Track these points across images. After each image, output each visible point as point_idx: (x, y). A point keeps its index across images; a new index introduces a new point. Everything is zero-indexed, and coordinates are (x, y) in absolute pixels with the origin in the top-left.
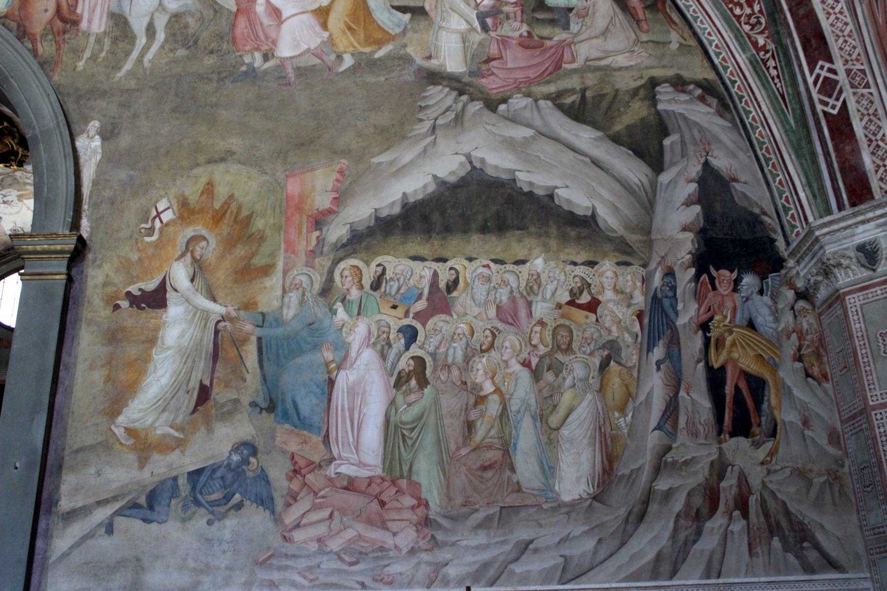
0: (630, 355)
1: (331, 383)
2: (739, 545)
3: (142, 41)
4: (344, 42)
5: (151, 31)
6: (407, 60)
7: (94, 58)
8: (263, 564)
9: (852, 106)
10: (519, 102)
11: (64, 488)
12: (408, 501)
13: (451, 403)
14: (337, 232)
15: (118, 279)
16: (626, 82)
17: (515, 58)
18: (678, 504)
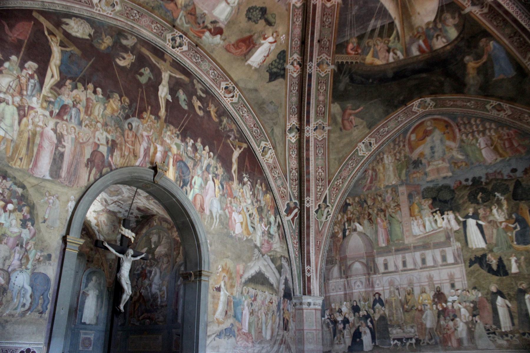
0: (275, 313)
1: (242, 313)
2: (284, 349)
3: (215, 220)
4: (245, 233)
5: (216, 217)
6: (252, 240)
7: (207, 222)
8: (234, 348)
9: (312, 277)
10: (266, 256)
11: (208, 330)
12: (251, 338)
13: (256, 319)
14: (243, 280)
15: (213, 283)
16: (279, 256)
17: (266, 245)
18: (279, 342)
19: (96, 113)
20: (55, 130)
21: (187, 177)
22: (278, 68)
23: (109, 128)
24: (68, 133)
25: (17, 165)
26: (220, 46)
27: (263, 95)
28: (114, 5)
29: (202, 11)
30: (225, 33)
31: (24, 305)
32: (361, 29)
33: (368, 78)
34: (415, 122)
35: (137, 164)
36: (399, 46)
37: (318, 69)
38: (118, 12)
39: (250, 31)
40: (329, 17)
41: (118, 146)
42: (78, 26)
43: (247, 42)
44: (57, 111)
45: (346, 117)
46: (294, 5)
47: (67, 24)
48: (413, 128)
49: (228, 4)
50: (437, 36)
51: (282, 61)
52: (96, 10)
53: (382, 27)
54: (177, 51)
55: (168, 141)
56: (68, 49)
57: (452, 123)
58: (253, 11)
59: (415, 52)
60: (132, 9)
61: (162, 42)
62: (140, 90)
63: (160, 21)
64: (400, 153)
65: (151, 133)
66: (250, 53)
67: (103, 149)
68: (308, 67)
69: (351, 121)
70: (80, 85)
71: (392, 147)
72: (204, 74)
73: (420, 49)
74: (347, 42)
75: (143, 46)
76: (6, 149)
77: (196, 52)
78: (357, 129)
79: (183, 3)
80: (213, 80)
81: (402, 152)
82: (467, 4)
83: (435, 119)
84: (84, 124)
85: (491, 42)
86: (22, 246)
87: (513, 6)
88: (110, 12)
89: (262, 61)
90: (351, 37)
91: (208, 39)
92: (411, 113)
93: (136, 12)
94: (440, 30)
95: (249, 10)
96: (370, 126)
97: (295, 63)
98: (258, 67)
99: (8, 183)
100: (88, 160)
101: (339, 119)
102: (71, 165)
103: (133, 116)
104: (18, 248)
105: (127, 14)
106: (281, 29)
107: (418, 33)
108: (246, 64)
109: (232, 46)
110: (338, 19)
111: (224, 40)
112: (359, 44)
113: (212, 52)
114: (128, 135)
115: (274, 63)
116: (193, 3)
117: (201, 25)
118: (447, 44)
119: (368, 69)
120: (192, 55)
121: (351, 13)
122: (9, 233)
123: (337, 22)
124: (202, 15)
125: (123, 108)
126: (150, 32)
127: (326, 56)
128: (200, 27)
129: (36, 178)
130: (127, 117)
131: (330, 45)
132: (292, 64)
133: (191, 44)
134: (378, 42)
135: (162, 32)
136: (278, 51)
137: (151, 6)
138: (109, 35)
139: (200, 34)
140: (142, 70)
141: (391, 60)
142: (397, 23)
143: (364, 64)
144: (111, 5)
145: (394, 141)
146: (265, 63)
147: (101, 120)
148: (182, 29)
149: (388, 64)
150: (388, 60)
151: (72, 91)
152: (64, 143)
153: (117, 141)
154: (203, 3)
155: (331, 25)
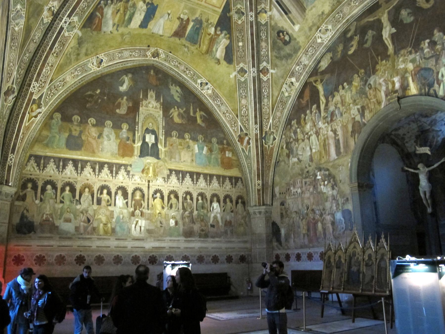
19: (347, 100)
20: (332, 130)
21: (431, 79)
23: (357, 101)
24: (338, 126)
25: (323, 161)
31: (343, 228)
35: (383, 106)
38: (332, 28)
41: (366, 107)
44: (330, 119)
52: (326, 42)
55: (402, 66)
56: (324, 80)
60: (334, 17)
62: (369, 53)
65: (386, 75)
67: (358, 118)
70: (336, 93)
75: (361, 20)
76: (317, 157)
84: (343, 113)
86: (335, 199)
88: (331, 33)
93: (337, 15)
99: (323, 172)
100: (352, 132)
102: (344, 142)
103: (369, 77)
104: (334, 201)
105: (336, 21)
114: (370, 93)
122: (328, 195)
125: (362, 79)
129: (331, 162)
130: (366, 81)
140: (366, 38)
144: (326, 31)
147: (351, 101)
151: (332, 101)
152: (337, 133)
153: (365, 105)
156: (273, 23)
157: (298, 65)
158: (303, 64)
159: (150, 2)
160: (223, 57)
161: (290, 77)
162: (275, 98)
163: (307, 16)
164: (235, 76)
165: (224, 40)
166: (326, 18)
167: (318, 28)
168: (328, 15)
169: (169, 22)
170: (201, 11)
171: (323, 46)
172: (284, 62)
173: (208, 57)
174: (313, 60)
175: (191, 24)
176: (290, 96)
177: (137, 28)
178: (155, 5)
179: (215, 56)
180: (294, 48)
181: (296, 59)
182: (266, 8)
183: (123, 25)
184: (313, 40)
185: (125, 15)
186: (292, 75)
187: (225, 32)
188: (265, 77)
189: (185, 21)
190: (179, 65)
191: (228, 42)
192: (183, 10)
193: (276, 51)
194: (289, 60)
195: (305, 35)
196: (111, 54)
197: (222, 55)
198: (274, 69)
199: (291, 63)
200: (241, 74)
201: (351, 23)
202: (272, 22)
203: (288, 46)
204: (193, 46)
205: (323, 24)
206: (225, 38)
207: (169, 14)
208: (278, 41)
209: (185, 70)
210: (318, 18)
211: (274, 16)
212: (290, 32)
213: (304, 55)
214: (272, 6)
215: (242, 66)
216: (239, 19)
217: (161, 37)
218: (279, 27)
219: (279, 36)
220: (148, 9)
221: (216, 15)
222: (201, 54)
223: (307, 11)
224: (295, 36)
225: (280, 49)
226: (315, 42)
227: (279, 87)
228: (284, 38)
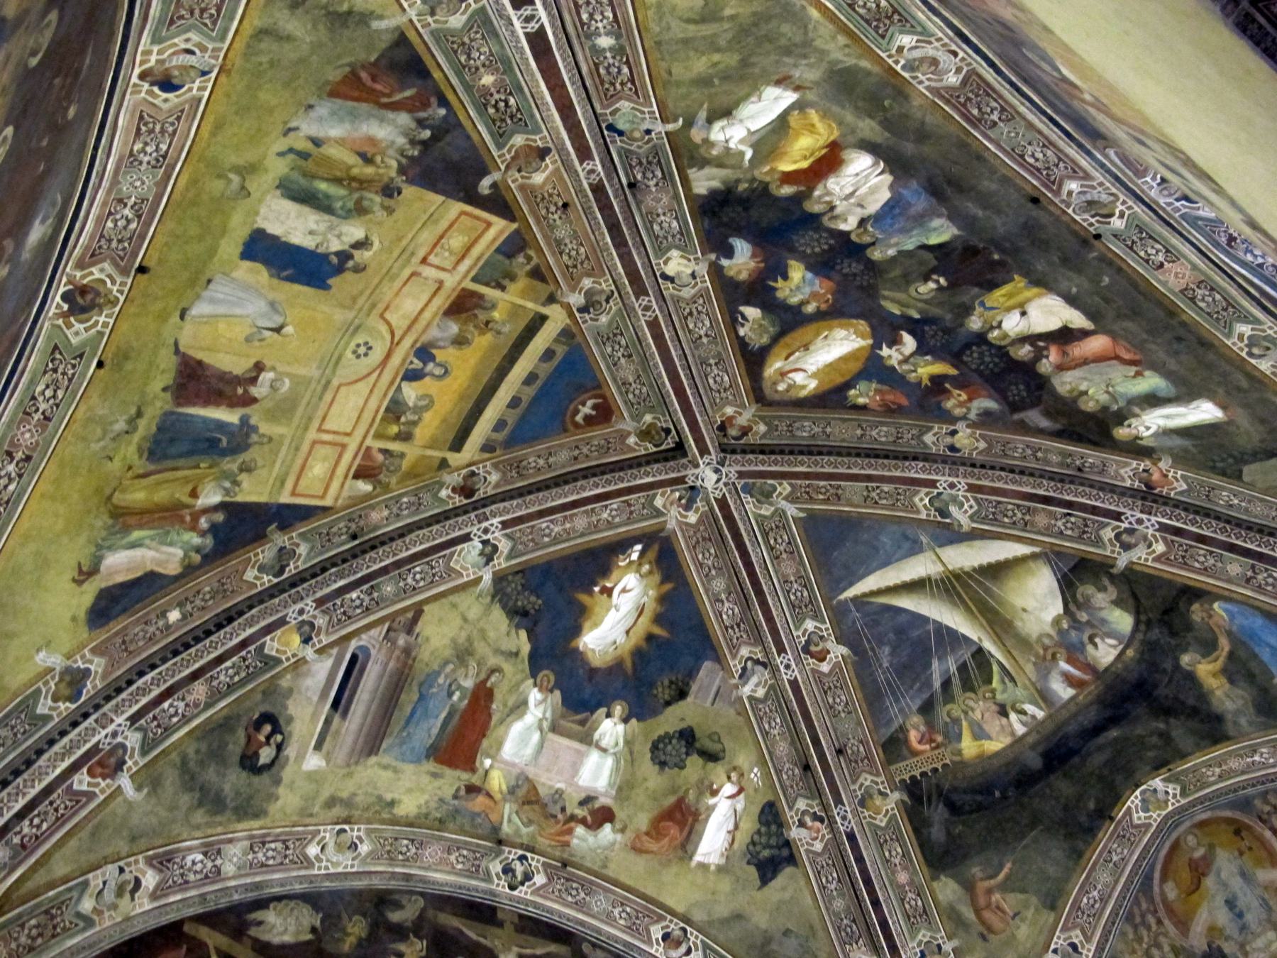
22: (771, 847)
26: (617, 846)
27: (761, 920)
28: (356, 846)
29: (551, 787)
30: (620, 814)
32: (920, 690)
33: (986, 789)
34: (1158, 850)
36: (1020, 692)
37: (866, 814)
39: (674, 790)
40: (839, 692)
42: (285, 919)
43: (678, 816)
45: (982, 901)
46: (750, 698)
47: (260, 923)
48: (1158, 867)
49: (604, 750)
50: (1091, 639)
51: (774, 828)
53: (963, 668)
54: (523, 892)
57: (1246, 820)
58: (665, 746)
59: (1064, 692)
60: (396, 839)
61: (483, 885)
63: (466, 843)
64: (1158, 946)
66: (693, 836)
68: (838, 819)
69: (998, 908)
71: (1131, 936)
72: (602, 921)
73: (1069, 680)
74: (903, 729)
75: (441, 910)
77: (568, 880)
78: (1023, 920)
79: (504, 787)
80: (630, 929)
81: (1162, 939)
82: (1113, 552)
83: (1202, 824)
85: (1216, 605)
87: (1207, 521)
89: (726, 845)
90: (906, 716)
91: (584, 840)
92: (1133, 831)
93: (405, 842)
94: (1088, 623)
95: (655, 748)
96: (1052, 902)
97: (808, 820)
98: (723, 861)
101: (969, 914)
105: (389, 852)
106: (743, 758)
107: (1046, 649)
108: (693, 864)
109: (645, 838)
110: (858, 692)
111: (623, 831)
112: (930, 725)
113: (605, 867)
115: (756, 838)
116: (527, 779)
117: (560, 816)
118: (1121, 647)
119: (980, 770)
120: (560, 891)
121: (881, 665)
123: (860, 696)
124: (553, 795)
126: (449, 873)
127: (870, 778)
128: (557, 822)
131: (868, 750)
132: (802, 824)
133: (550, 866)
134: (971, 703)
135: (477, 862)
136: (756, 810)
137: (435, 819)
138: (356, 912)
139: (562, 838)
141: (1020, 730)
142: (988, 645)
143: (963, 764)
144: (349, 848)
145: (1129, 918)
146: (736, 846)
148: (519, 841)
149: (1019, 741)
150: (1013, 733)
154: (548, 770)
155: (850, 707)
156: (285, 683)
157: (205, 854)
158: (218, 862)
159: (350, 264)
160: (110, 583)
161: (149, 862)
162: (40, 878)
163: (360, 768)
164: (50, 670)
165: (180, 553)
166: (383, 822)
167: (347, 821)
168: (394, 822)
169: (240, 331)
170: (282, 436)
171: (303, 873)
172: (185, 799)
173: (99, 523)
174: (249, 880)
175: (227, 416)
176: (89, 922)
177: (255, 222)
178: (330, 281)
179: (110, 548)
180: (251, 797)
181: (219, 829)
182: (318, 634)
183: (295, 176)
184: (304, 833)
185: (337, 181)
186: (162, 862)
187: (209, 541)
188: (87, 779)
189: (246, 391)
190: (37, 416)
191: (173, 569)
192: (288, 375)
193: (204, 747)
194: (200, 812)
195: (306, 800)
196: (182, 126)
197: (117, 572)
198: (139, 788)
199: (198, 827)
200: (63, 685)
201: (412, 893)
202: (289, 676)
203: (244, 774)
204: (140, 450)
205: (363, 827)
206: (186, 555)
207: (278, 330)
208: (241, 735)
209: (19, 455)
210: (373, 799)
211: (309, 670)
212: (290, 751)
213: (247, 843)
214: (335, 651)
215: (92, 668)
216: (262, 569)
217: (178, 313)
218: (286, 708)
219: (258, 725)
220: (325, 256)
221: (269, 488)
222: (108, 491)
223: (373, 759)
224: (287, 774)
225: (217, 755)
226: (303, 840)
227: (93, 858)
228: (261, 745)
